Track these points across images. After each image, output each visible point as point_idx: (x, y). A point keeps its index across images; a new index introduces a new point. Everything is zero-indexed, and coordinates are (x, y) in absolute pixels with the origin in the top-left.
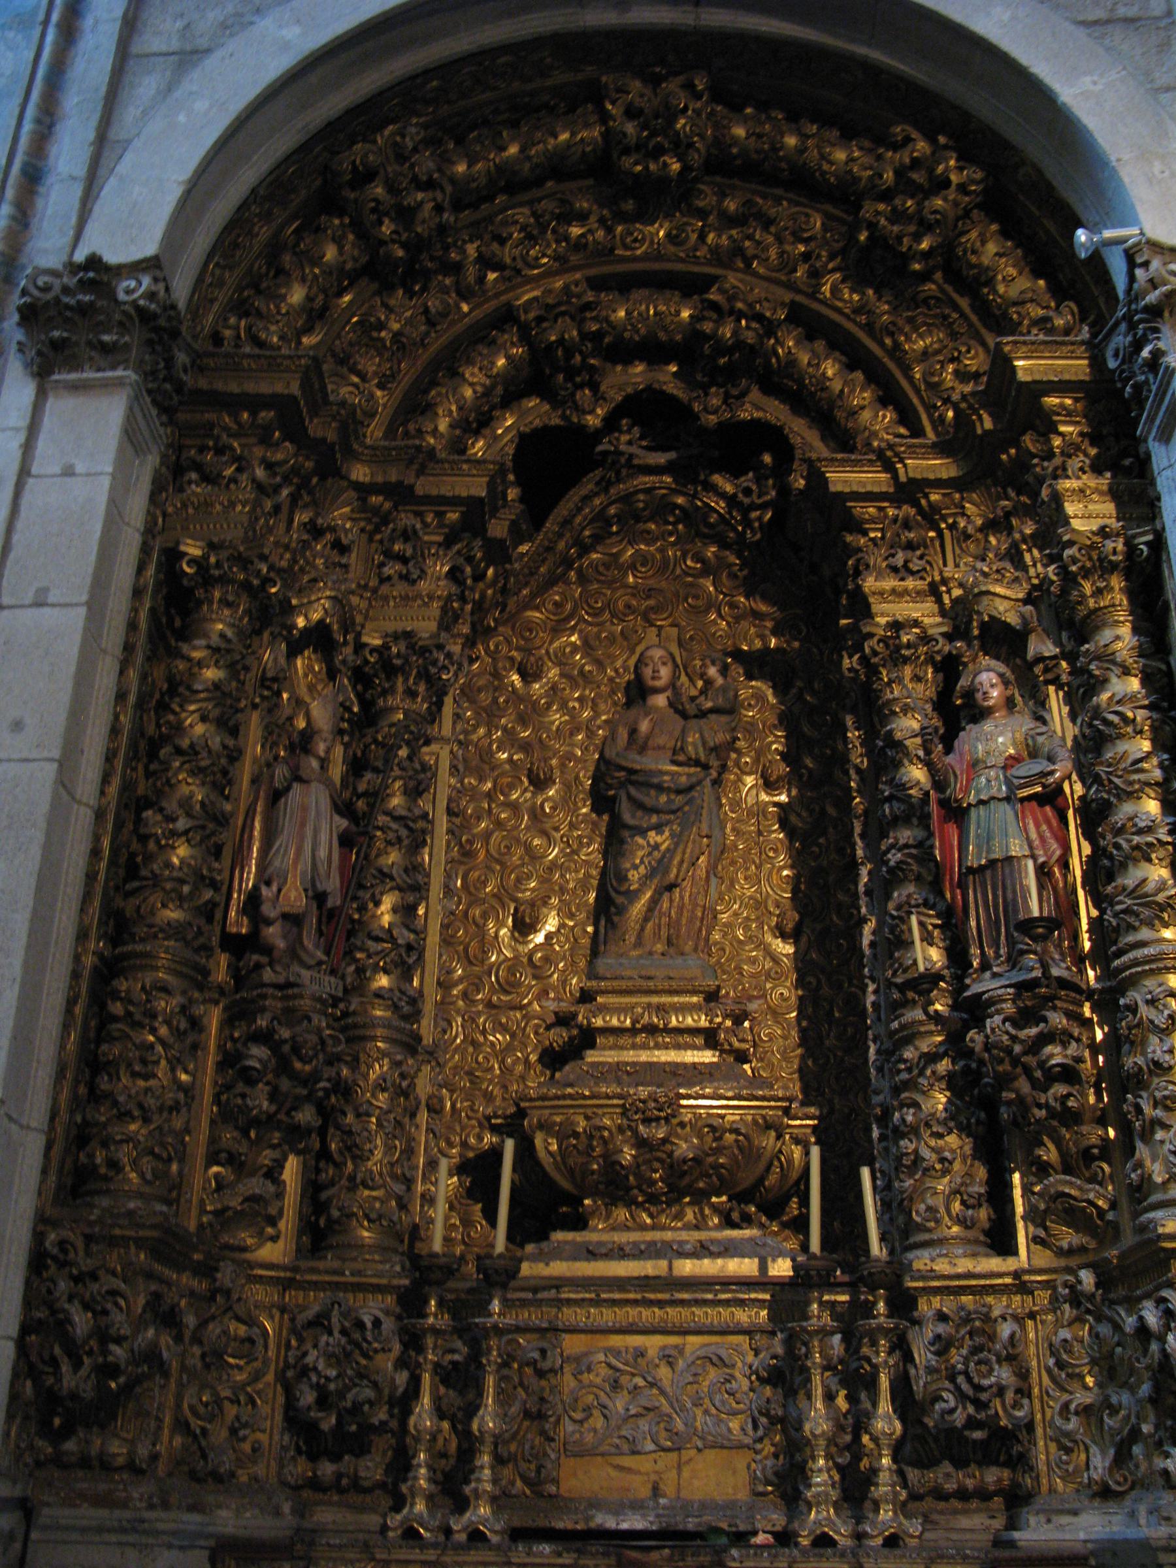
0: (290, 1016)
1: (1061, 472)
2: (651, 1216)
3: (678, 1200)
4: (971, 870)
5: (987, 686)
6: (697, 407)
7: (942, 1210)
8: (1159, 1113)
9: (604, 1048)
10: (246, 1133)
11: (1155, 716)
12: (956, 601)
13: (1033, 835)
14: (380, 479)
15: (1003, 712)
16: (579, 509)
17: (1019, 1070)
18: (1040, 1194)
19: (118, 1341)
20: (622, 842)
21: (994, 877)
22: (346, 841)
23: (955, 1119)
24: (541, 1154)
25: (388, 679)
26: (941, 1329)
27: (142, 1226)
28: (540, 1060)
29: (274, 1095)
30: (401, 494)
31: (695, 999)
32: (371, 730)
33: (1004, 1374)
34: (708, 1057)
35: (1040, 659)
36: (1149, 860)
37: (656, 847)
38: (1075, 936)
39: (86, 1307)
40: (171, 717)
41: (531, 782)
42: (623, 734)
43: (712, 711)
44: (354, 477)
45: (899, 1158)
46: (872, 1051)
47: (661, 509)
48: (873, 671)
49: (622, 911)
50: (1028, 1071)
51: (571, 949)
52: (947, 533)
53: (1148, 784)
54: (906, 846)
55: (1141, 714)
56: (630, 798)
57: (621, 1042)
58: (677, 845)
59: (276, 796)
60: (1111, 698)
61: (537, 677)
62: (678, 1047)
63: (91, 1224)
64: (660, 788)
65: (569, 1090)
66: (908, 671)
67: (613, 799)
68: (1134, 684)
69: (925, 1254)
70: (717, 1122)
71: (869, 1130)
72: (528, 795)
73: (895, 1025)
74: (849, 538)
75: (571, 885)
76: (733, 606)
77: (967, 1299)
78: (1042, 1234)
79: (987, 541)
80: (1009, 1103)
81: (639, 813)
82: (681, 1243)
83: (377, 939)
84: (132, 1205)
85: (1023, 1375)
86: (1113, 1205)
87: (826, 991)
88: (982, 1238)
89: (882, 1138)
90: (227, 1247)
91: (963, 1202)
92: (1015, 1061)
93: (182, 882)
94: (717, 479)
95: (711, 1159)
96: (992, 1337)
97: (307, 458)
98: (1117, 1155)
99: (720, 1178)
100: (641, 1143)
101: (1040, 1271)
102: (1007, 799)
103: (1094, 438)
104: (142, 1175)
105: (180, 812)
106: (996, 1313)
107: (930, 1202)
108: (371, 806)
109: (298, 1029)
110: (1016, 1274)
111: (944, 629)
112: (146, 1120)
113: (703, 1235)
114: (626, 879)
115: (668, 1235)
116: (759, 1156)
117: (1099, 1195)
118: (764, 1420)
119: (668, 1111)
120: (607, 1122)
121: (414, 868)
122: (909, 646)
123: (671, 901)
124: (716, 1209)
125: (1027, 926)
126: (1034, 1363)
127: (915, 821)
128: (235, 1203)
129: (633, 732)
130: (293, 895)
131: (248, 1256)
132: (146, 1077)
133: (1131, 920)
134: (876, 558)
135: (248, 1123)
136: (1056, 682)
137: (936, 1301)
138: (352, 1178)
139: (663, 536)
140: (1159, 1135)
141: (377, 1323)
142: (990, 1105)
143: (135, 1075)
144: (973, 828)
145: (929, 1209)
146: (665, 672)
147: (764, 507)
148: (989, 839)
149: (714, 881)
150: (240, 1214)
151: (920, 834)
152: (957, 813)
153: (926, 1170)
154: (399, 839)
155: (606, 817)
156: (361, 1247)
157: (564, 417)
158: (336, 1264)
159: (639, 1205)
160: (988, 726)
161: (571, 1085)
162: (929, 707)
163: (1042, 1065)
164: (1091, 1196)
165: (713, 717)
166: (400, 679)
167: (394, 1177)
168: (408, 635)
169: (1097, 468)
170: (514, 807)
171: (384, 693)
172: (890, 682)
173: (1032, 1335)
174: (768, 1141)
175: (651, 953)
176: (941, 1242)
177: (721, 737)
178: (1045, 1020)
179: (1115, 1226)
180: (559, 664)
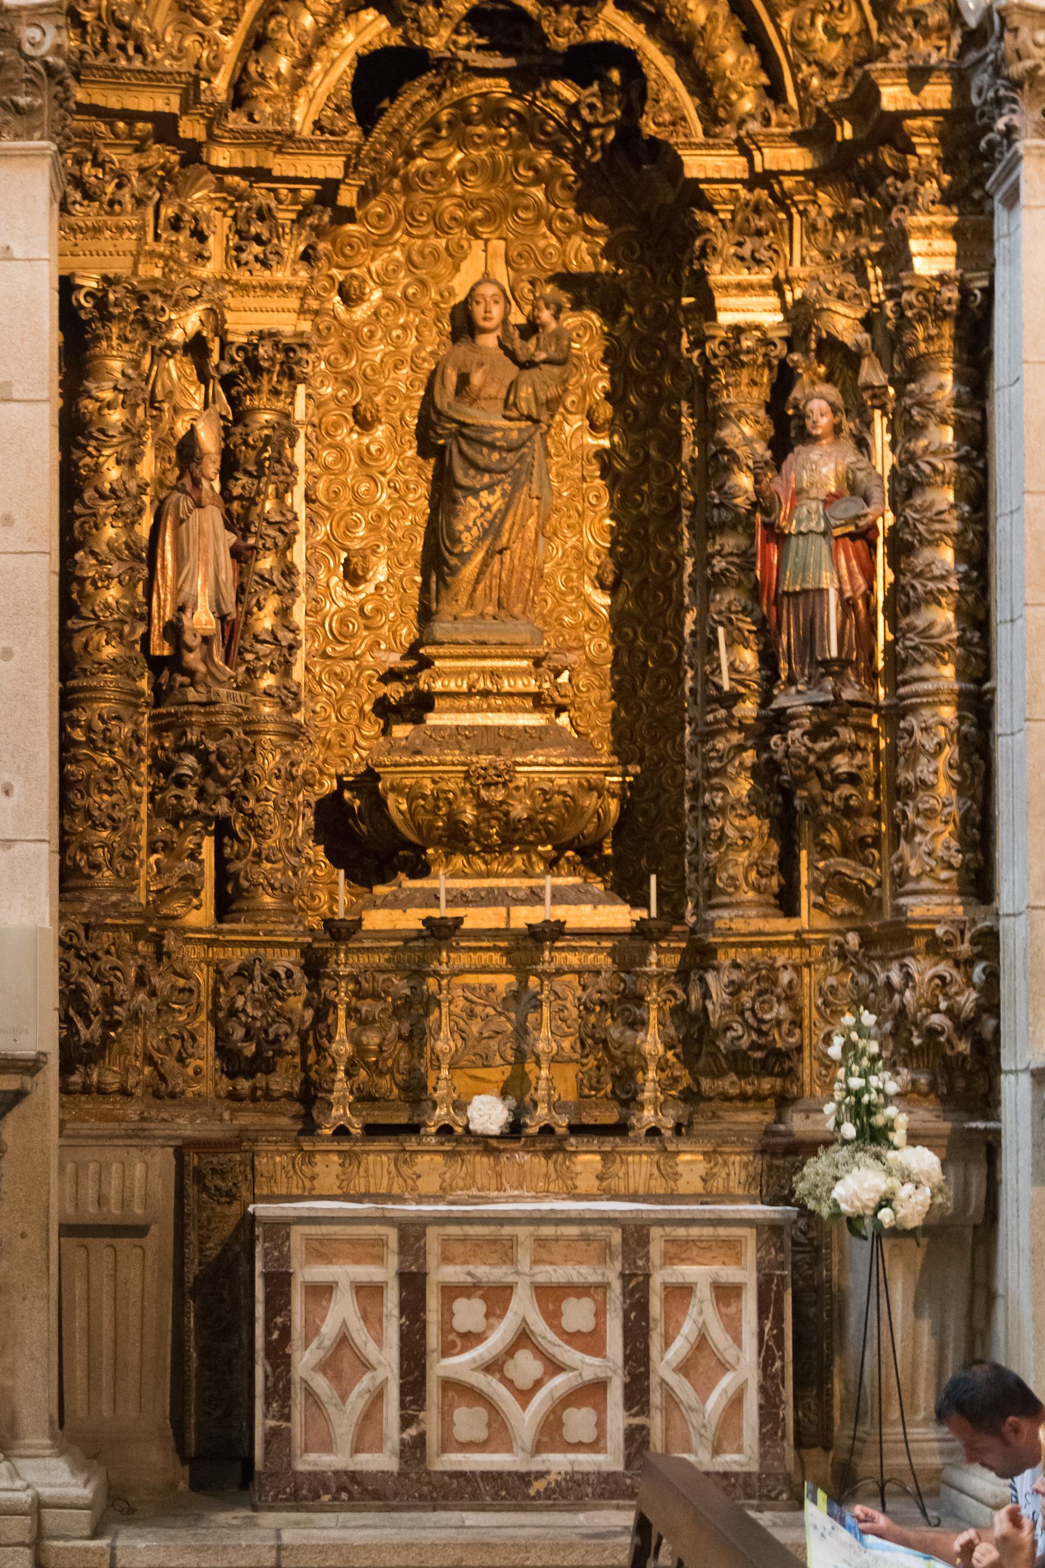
0: (213, 729)
1: (909, 201)
2: (486, 863)
3: (510, 850)
4: (787, 594)
5: (817, 413)
6: (547, 28)
7: (741, 877)
8: (919, 821)
9: (442, 711)
10: (176, 825)
11: (963, 468)
12: (797, 303)
13: (844, 571)
14: (238, 163)
15: (830, 439)
16: (409, 116)
17: (812, 774)
18: (822, 871)
19: (121, 1003)
20: (455, 501)
21: (806, 603)
22: (236, 553)
23: (756, 804)
24: (397, 818)
25: (255, 380)
26: (736, 975)
27: (127, 915)
28: (374, 710)
29: (201, 794)
30: (259, 174)
31: (524, 663)
32: (239, 429)
33: (781, 1011)
34: (535, 720)
35: (869, 387)
36: (939, 604)
37: (488, 508)
38: (872, 656)
39: (96, 980)
40: (87, 460)
41: (356, 422)
42: (452, 377)
43: (544, 362)
44: (214, 162)
45: (706, 836)
46: (688, 731)
47: (494, 112)
48: (711, 371)
49: (454, 571)
50: (820, 774)
51: (401, 600)
52: (797, 218)
53: (947, 534)
54: (731, 554)
55: (950, 467)
56: (461, 452)
57: (457, 703)
58: (508, 506)
59: (179, 522)
60: (926, 448)
61: (361, 298)
62: (510, 710)
63: (86, 915)
64: (492, 446)
65: (418, 758)
66: (745, 375)
67: (443, 448)
68: (948, 435)
69: (725, 913)
70: (546, 786)
71: (680, 803)
72: (355, 436)
73: (710, 718)
74: (699, 216)
75: (399, 534)
76: (563, 219)
77: (756, 951)
78: (820, 900)
79: (835, 236)
80: (802, 798)
81: (472, 472)
82: (516, 889)
83: (264, 642)
84: (114, 898)
85: (797, 1011)
86: (879, 884)
87: (641, 641)
88: (772, 901)
89: (692, 809)
90: (166, 917)
91: (759, 872)
92: (810, 768)
93: (123, 622)
94: (558, 86)
95: (541, 817)
96: (775, 982)
97: (174, 152)
98: (885, 844)
99: (548, 831)
100: (482, 805)
101: (817, 931)
102: (824, 534)
103: (948, 163)
104: (117, 873)
105: (112, 557)
106: (779, 963)
107: (731, 872)
108: (247, 510)
109: (222, 742)
110: (797, 933)
111: (785, 333)
112: (115, 829)
113: (533, 882)
114: (459, 541)
115: (503, 882)
116: (583, 814)
117: (868, 875)
118: (590, 1041)
119: (503, 778)
120: (452, 786)
121: (288, 571)
122: (749, 351)
123: (502, 563)
124: (541, 856)
125: (826, 663)
126: (807, 1002)
127: (740, 529)
128: (174, 883)
129: (464, 380)
130: (204, 618)
131: (178, 922)
132: (110, 793)
133: (917, 656)
134: (724, 242)
135: (176, 817)
136: (882, 407)
137: (732, 952)
138: (258, 854)
139: (494, 140)
140: (918, 838)
141: (289, 974)
142: (788, 795)
143: (101, 791)
144: (792, 554)
145: (730, 877)
146: (497, 312)
147: (606, 126)
148: (805, 568)
149: (541, 540)
150: (174, 891)
151: (742, 541)
152: (778, 537)
153: (729, 845)
154: (276, 545)
155: (432, 461)
156: (262, 910)
157: (405, 37)
158: (250, 927)
159: (475, 853)
160: (815, 453)
161: (418, 753)
162: (762, 413)
163: (832, 771)
164: (863, 876)
165: (545, 367)
166: (265, 378)
167: (289, 850)
168: (272, 335)
169: (948, 198)
170: (339, 448)
171: (251, 392)
172: (727, 386)
173: (806, 980)
174: (590, 802)
175: (482, 615)
176: (738, 904)
177: (553, 392)
178: (837, 734)
179: (880, 902)
180: (382, 284)
